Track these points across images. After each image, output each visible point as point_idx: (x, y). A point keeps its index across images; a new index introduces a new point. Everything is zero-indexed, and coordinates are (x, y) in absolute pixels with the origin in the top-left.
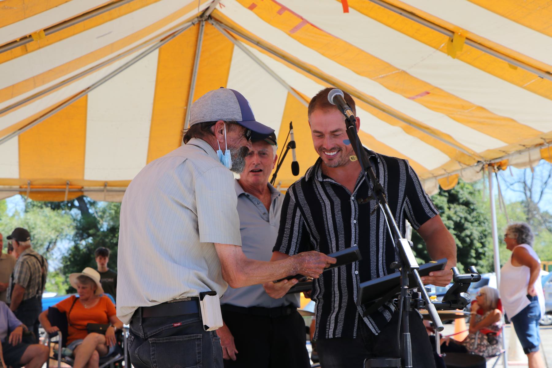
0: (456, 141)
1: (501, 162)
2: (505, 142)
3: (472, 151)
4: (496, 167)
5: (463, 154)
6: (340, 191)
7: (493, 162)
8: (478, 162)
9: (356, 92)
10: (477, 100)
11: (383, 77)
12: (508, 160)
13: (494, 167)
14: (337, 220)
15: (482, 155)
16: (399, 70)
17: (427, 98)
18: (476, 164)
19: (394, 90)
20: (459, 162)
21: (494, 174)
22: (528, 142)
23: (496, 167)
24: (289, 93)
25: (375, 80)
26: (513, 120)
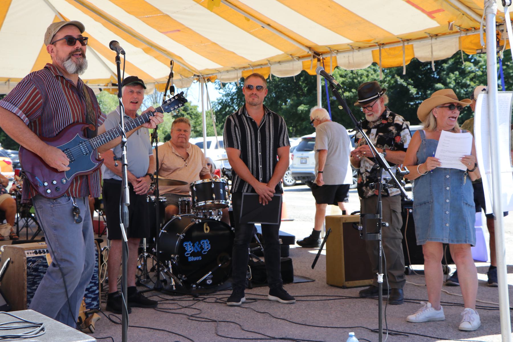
0: (185, 62)
1: (210, 77)
2: (222, 65)
3: (195, 69)
4: (206, 80)
5: (185, 69)
6: (254, 124)
7: (205, 76)
8: (195, 75)
9: (117, 22)
10: (212, 38)
11: (148, 17)
12: (216, 76)
13: (205, 79)
14: (253, 138)
15: (201, 72)
16: (164, 13)
17: (178, 33)
18: (192, 77)
19: (153, 26)
20: (181, 75)
21: (205, 84)
22: (237, 66)
23: (206, 80)
24: (56, 16)
25: (139, 18)
26: (234, 53)
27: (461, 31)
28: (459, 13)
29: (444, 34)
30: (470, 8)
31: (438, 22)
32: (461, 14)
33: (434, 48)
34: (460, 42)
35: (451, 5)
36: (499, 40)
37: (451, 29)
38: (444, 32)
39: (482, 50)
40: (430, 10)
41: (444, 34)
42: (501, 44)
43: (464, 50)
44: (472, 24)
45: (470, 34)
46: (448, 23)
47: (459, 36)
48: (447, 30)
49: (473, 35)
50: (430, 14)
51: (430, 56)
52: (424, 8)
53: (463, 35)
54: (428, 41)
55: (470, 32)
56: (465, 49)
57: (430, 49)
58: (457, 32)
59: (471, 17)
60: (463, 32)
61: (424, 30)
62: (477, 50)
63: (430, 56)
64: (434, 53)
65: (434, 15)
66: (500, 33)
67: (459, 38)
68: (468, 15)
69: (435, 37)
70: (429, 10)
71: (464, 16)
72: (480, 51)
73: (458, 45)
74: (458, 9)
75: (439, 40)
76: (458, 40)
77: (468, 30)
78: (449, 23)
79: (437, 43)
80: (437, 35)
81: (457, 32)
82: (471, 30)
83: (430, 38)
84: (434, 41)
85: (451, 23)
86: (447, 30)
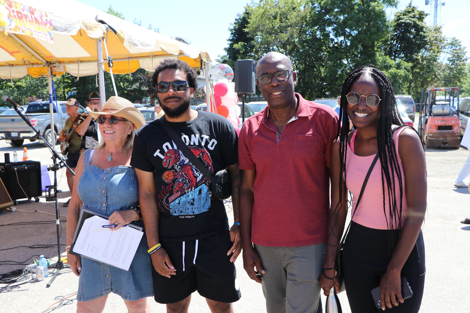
27: (29, 64)
28: (30, 54)
29: (17, 65)
30: (37, 53)
31: (16, 58)
32: (31, 55)
33: (11, 71)
34: (28, 70)
35: (26, 50)
36: (52, 71)
37: (25, 62)
38: (18, 64)
39: (42, 76)
40: (12, 51)
41: (17, 65)
42: (53, 73)
43: (32, 75)
44: (36, 61)
45: (34, 66)
46: (22, 59)
47: (28, 67)
48: (22, 63)
49: (36, 67)
50: (11, 53)
51: (10, 76)
52: (8, 49)
53: (31, 66)
54: (8, 68)
55: (35, 65)
56: (32, 74)
57: (9, 72)
58: (28, 64)
59: (37, 57)
60: (30, 65)
61: (4, 62)
62: (39, 75)
63: (10, 76)
64: (12, 75)
65: (13, 54)
66: (52, 67)
67: (28, 68)
68: (36, 56)
69: (11, 66)
70: (11, 51)
71: (33, 57)
72: (41, 76)
73: (27, 72)
74: (30, 53)
75: (14, 67)
76: (26, 69)
77: (33, 64)
78: (23, 59)
79: (13, 69)
80: (12, 65)
81: (28, 64)
82: (36, 64)
83: (9, 66)
84: (11, 67)
85: (24, 59)
86: (22, 63)
